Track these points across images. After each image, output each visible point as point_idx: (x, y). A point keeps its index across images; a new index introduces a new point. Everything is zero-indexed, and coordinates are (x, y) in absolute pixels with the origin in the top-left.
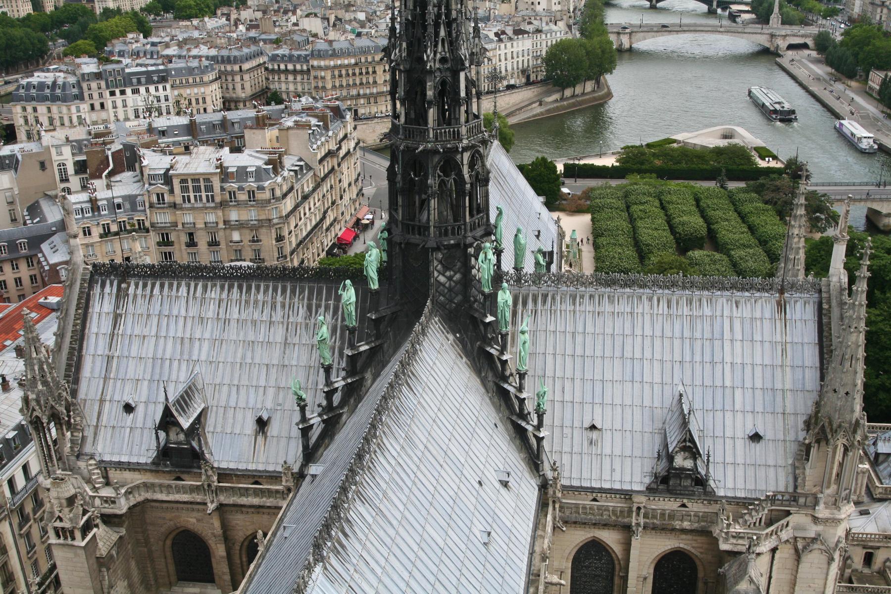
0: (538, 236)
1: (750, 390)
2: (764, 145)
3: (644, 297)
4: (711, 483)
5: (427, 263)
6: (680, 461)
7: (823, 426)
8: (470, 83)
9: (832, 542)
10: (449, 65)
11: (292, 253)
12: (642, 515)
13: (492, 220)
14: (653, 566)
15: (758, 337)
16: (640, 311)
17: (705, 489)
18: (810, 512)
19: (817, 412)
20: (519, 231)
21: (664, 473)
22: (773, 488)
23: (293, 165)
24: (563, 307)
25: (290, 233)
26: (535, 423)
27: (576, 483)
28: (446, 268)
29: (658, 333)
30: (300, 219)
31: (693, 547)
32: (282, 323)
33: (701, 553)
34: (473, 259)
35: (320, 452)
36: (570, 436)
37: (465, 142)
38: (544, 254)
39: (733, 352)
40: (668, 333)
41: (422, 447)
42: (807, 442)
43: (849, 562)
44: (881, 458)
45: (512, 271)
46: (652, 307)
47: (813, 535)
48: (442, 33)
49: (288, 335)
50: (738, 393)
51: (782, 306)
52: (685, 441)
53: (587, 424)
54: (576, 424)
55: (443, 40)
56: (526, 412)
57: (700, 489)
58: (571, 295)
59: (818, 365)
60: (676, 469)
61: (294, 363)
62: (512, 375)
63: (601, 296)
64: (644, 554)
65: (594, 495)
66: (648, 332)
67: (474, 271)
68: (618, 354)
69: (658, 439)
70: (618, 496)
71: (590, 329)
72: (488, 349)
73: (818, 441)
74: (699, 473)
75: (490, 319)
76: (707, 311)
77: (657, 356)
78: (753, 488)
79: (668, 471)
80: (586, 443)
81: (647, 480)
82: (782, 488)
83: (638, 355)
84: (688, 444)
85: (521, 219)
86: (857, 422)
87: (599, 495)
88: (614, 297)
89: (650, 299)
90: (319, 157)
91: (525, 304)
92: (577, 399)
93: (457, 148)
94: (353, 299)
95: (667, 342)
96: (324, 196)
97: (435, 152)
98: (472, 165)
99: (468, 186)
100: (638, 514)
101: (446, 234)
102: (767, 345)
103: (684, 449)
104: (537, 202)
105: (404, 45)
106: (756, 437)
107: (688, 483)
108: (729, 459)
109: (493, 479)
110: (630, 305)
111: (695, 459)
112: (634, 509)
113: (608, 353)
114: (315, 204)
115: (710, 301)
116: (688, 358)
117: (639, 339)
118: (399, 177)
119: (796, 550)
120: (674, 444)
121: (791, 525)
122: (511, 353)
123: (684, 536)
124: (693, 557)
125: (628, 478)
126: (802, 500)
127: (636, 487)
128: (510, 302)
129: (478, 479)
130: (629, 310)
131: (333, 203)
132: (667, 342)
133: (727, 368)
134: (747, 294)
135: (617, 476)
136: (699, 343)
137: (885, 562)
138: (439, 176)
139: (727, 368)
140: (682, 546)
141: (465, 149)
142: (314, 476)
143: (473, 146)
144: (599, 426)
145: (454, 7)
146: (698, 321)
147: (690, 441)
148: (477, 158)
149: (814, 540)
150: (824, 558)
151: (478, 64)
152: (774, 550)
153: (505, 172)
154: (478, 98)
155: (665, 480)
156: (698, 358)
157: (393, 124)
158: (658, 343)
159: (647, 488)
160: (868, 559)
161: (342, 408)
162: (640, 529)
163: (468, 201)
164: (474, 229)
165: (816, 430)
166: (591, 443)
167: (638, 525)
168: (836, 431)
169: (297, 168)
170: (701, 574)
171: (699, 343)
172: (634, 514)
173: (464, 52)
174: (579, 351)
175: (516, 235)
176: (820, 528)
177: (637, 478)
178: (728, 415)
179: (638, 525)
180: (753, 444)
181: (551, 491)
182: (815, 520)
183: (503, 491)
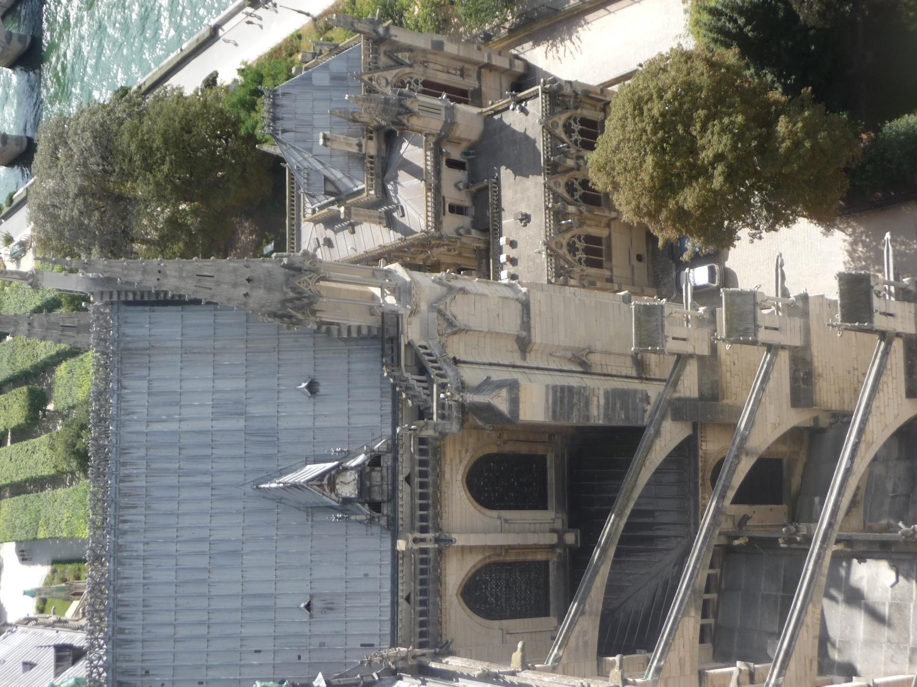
1: (249, 395)
3: (120, 541)
6: (348, 488)
9: (439, 290)
12: (424, 536)
14: (489, 512)
15: (175, 386)
16: (141, 546)
18: (405, 320)
19: (274, 315)
21: (366, 509)
27: (387, 629)
29: (172, 520)
31: (461, 462)
43: (462, 231)
44: (330, 188)
46: (134, 531)
47: (435, 314)
50: (254, 410)
52: (321, 486)
54: (305, 629)
57: (387, 461)
63: (119, 603)
64: (473, 529)
65: (400, 600)
66: (172, 533)
68: (205, 575)
69: (320, 517)
70: (400, 568)
71: (168, 617)
73: (314, 312)
74: (363, 463)
76: (142, 452)
78: (379, 391)
79: (363, 504)
80: (331, 616)
81: (376, 529)
82: (379, 354)
83: (205, 547)
84: (325, 482)
87: (400, 594)
88: (121, 586)
89: (124, 533)
92: (270, 630)
95: (185, 508)
100: (423, 540)
102: (185, 373)
106: (312, 388)
107: (376, 475)
108: (342, 422)
110: (134, 562)
112: (416, 547)
113: (204, 589)
115: (123, 451)
116: (207, 479)
117: (179, 547)
119: (455, 333)
120: (328, 500)
121: (424, 343)
123: (447, 476)
126: (392, 332)
127: (388, 545)
130: (140, 563)
132: (185, 508)
133: (219, 425)
135: (374, 572)
136: (184, 465)
139: (219, 425)
140: (459, 477)
146: (154, 466)
147: (322, 480)
149: (439, 312)
150: (460, 298)
155: (376, 507)
159: (388, 529)
160: (456, 209)
162: (443, 537)
165: (300, 316)
166: (331, 609)
167: (437, 540)
168: (300, 293)
170: (494, 450)
171: (184, 465)
172: (423, 546)
174: (203, 630)
176: (424, 307)
178: (283, 424)
179: (437, 540)
180: (322, 390)
181: (400, 664)
182: (413, 313)
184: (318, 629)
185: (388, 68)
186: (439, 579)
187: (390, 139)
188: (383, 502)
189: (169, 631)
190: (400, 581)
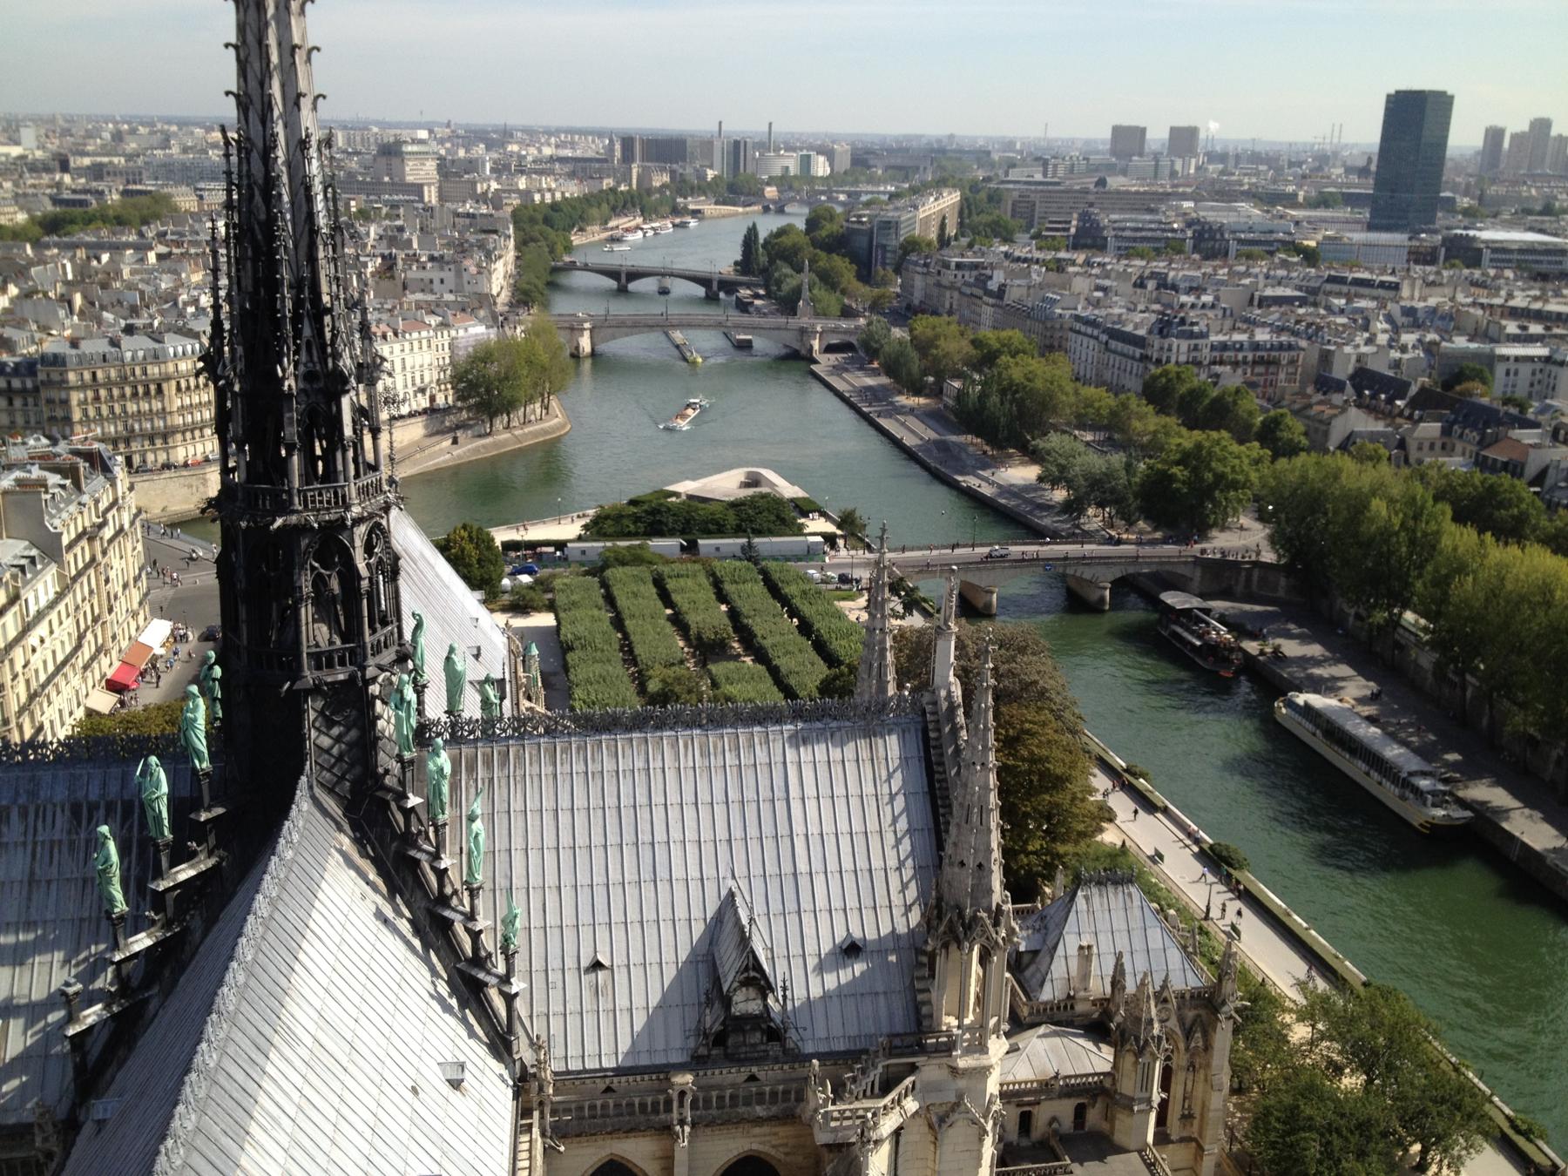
0: (477, 656)
4: (792, 1034)
5: (300, 714)
7: (951, 920)
8: (360, 412)
10: (321, 385)
11: (20, 713)
13: (408, 636)
17: (783, 1046)
18: (945, 1060)
20: (452, 650)
21: (717, 1027)
22: (885, 1030)
23: (15, 557)
25: (15, 677)
26: (501, 969)
28: (330, 724)
30: (34, 650)
32: (24, 844)
33: (787, 1154)
34: (378, 703)
35: (108, 1076)
36: (560, 984)
37: (356, 510)
40: (704, 796)
41: (308, 1041)
42: (929, 948)
44: (1026, 959)
45: (444, 718)
47: (953, 1100)
48: (307, 332)
49: (37, 865)
52: (747, 969)
53: (585, 963)
55: (309, 344)
56: (483, 954)
57: (774, 1049)
59: (931, 825)
60: (737, 1018)
61: (49, 916)
62: (455, 892)
65: (608, 1081)
66: (673, 798)
67: (381, 724)
72: (412, 853)
77: (691, 835)
79: (723, 1023)
81: (692, 1043)
82: (899, 1029)
84: (752, 974)
85: (454, 630)
90: (65, 541)
93: (343, 519)
94: (165, 788)
96: (77, 608)
97: (304, 528)
98: (369, 549)
99: (365, 584)
100: (681, 1105)
101: (330, 665)
103: (747, 983)
104: (468, 600)
105: (240, 350)
107: (756, 1037)
109: (435, 1080)
111: (765, 998)
112: (675, 1095)
114: (61, 623)
116: (737, 833)
118: (241, 573)
120: (730, 979)
122: (452, 855)
123: (757, 1130)
124: (774, 1163)
125: (660, 1045)
127: (676, 1058)
128: (448, 770)
129: (410, 1084)
130: (639, 764)
131: (95, 620)
134: (819, 725)
137: (1050, 1124)
138: (313, 568)
140: (755, 1147)
141: (358, 521)
142: (101, 1123)
143: (371, 516)
144: (605, 961)
145: (324, 288)
147: (754, 969)
148: (378, 534)
151: (371, 383)
152: (897, 1133)
153: (416, 555)
154: (375, 438)
155: (720, 1039)
156: (753, 831)
157: (223, 483)
158: (689, 812)
161: (148, 988)
163: (364, 607)
164: (379, 652)
165: (942, 929)
169: (23, 562)
172: (675, 1104)
173: (346, 363)
175: (448, 659)
177: (677, 1042)
183: (454, 1096)
184: (571, 978)
185: (1181, 1020)
186: (632, 1131)
187: (1097, 1029)
188: (726, 1048)
190: (631, 1078)
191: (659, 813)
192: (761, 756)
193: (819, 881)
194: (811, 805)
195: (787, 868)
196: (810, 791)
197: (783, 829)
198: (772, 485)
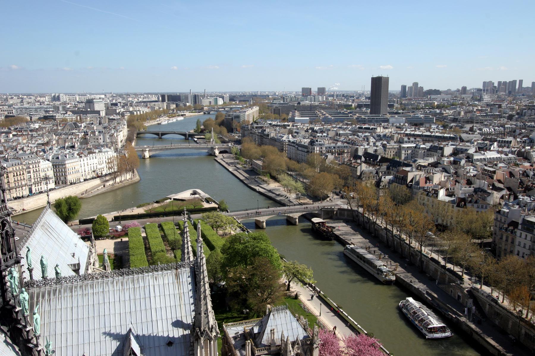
2: (209, 197)
24: (66, 295)
29: (117, 299)
38: (74, 265)
39: (156, 303)
40: (122, 299)
51: (177, 276)
58: (69, 288)
66: (112, 300)
67: (8, 284)
75: (18, 309)
77: (117, 311)
86: (212, 326)
91: (43, 297)
116: (133, 309)
130: (101, 290)
158: (117, 304)
175: (41, 260)
180: (169, 348)
189: (75, 305)
191: (107, 305)
192: (142, 284)
193: (160, 323)
194: (158, 299)
195: (149, 319)
196: (157, 294)
197: (148, 307)
198: (199, 194)
